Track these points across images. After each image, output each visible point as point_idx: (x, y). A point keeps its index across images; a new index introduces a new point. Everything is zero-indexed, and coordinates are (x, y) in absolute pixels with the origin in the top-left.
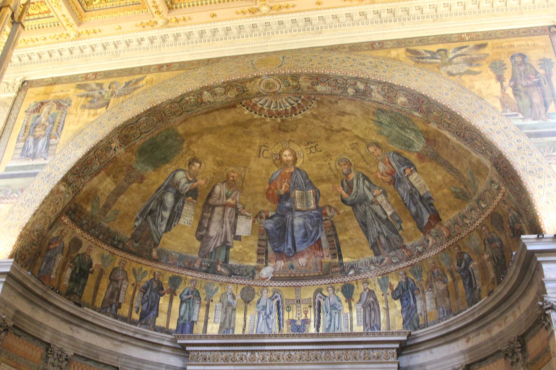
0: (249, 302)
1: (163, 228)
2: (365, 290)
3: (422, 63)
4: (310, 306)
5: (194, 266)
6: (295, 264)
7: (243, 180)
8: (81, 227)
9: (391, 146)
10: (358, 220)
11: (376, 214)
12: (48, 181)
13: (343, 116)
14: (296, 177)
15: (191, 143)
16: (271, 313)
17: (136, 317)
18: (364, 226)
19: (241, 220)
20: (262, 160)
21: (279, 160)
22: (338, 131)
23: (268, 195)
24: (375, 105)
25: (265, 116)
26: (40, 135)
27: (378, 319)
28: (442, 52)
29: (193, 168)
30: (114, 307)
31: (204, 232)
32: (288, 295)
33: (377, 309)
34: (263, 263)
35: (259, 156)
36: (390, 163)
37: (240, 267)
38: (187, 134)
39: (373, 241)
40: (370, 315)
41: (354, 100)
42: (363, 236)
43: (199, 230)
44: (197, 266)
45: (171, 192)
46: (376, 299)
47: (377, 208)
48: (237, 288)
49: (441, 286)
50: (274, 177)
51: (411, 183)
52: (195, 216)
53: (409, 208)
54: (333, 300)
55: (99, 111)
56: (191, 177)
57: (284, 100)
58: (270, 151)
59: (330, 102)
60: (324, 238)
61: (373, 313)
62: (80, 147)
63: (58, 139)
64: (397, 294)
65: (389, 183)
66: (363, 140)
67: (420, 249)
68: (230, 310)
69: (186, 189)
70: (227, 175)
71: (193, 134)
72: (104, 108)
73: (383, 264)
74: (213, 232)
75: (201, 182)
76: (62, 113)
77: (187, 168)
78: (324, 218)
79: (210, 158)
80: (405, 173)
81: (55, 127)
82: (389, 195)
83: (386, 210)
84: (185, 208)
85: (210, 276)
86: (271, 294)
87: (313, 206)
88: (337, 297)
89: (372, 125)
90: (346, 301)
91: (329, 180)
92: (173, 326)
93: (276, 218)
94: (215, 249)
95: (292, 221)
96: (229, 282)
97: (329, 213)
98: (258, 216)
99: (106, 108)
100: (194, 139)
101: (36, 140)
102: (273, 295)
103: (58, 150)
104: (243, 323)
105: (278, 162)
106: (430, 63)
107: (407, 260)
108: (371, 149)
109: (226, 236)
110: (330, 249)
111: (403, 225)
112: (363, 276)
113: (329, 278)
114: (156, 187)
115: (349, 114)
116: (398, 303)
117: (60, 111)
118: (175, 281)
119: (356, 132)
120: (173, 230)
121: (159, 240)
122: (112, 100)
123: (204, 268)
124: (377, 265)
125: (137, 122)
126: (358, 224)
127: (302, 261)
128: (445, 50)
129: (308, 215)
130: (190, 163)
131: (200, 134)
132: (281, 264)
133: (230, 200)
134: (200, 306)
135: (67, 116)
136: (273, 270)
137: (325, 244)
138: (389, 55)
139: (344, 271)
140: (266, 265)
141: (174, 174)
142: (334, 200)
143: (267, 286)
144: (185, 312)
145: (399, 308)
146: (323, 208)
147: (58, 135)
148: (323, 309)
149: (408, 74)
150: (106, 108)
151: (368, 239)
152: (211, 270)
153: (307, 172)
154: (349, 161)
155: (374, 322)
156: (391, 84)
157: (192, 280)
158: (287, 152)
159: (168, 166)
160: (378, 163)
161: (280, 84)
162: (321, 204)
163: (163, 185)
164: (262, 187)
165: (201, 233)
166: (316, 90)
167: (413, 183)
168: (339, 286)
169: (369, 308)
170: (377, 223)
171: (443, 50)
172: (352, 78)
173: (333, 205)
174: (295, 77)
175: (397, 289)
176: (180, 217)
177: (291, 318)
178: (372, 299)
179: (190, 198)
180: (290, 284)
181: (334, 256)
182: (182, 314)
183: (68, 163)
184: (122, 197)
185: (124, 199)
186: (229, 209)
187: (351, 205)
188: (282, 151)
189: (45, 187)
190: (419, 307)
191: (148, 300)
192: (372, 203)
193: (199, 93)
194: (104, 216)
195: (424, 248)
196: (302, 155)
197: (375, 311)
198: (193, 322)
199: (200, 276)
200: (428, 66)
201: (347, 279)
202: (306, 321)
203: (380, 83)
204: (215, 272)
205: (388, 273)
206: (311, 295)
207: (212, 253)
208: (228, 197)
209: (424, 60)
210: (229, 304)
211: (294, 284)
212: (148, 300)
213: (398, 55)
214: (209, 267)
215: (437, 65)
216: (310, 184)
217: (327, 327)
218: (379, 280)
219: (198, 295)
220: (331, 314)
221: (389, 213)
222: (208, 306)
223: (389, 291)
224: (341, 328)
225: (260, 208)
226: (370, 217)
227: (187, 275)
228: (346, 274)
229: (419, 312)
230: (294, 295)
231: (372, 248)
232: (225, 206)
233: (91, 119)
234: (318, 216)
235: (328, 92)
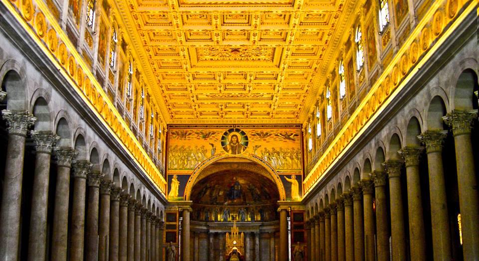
18: (252, 194)
21: (232, 179)
49: (270, 212)
74: (213, 195)
87: (239, 188)
92: (204, 219)
118: (204, 208)
120: (205, 196)
127: (235, 201)
132: (230, 201)
137: (242, 197)
139: (246, 205)
152: (212, 204)
201: (247, 206)
202: (236, 216)
219: (209, 210)
221: (259, 193)
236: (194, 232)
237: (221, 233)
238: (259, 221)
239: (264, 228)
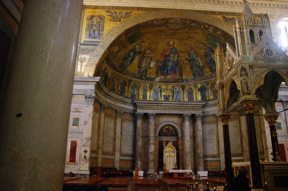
0: (151, 89)
1: (128, 64)
2: (189, 87)
3: (227, 22)
4: (170, 91)
5: (136, 77)
6: (167, 77)
7: (156, 49)
8: (107, 63)
9: (208, 45)
10: (190, 66)
11: (197, 65)
12: (103, 48)
13: (195, 33)
14: (173, 50)
15: (143, 36)
16: (158, 93)
17: (119, 93)
18: (192, 68)
19: (152, 62)
20: (163, 44)
21: (168, 44)
22: (192, 38)
23: (162, 55)
24: (208, 33)
25: (169, 30)
26: (95, 30)
27: (193, 97)
28: (233, 19)
29: (142, 44)
30: (114, 90)
31: (140, 65)
32: (164, 87)
33: (192, 94)
34: (156, 76)
35: (162, 42)
36: (206, 51)
37: (150, 77)
38: (143, 33)
39: (194, 73)
40: (190, 95)
41: (202, 30)
42: (191, 71)
43: (139, 65)
44: (137, 76)
45: (133, 52)
46: (192, 91)
47: (197, 63)
48: (148, 84)
50: (165, 49)
51: (211, 57)
52: (138, 60)
53: (209, 64)
54: (178, 90)
55: (117, 23)
56: (140, 47)
57: (178, 26)
58: (166, 41)
59: (193, 29)
60: (177, 70)
61: (191, 95)
62: (113, 36)
63: (103, 32)
64: (200, 90)
65: (204, 56)
66: (199, 42)
67: (209, 77)
68: (145, 91)
69: (138, 51)
70: (151, 47)
71: (145, 33)
72: (119, 22)
73: (196, 80)
74: (143, 66)
75: (143, 49)
76: (102, 21)
77: (140, 44)
78: (179, 64)
79: (147, 41)
80: (210, 54)
81: (101, 27)
82: (202, 59)
83: (200, 64)
84: (136, 57)
85: (140, 80)
86: (158, 87)
87: (176, 60)
88: (180, 89)
89: (204, 38)
90: (182, 90)
91: (183, 52)
92: (130, 96)
93: (163, 62)
94: (143, 71)
95: (168, 64)
96: (146, 82)
97: (181, 63)
98: (158, 61)
99: (120, 22)
100: (145, 35)
101: (94, 31)
102: (159, 87)
103: (104, 37)
104: (149, 95)
105: (168, 44)
106: (230, 22)
107: (204, 80)
108: (201, 45)
109: (147, 67)
110: (179, 74)
111: (205, 69)
112: (189, 83)
113: (177, 83)
114: (129, 50)
115: (198, 33)
116: (200, 92)
117: (101, 21)
118: (130, 81)
119: (198, 39)
120: (131, 64)
121: (127, 68)
122: (122, 19)
123: (139, 77)
124: (194, 80)
125: (131, 29)
126: (190, 67)
127: (169, 77)
128: (234, 18)
129: (174, 63)
130: (141, 43)
131: (147, 33)
132: (162, 77)
133: (150, 56)
134: (137, 90)
135: (105, 23)
136: (159, 79)
137: (177, 72)
138: (217, 17)
139: (183, 81)
140: (158, 77)
141: (135, 46)
142: (183, 59)
143: (157, 84)
144: (132, 91)
145: (200, 94)
146: (179, 61)
147: (103, 30)
148: (175, 92)
149: (223, 25)
150: (120, 22)
151: (192, 72)
152: (141, 78)
153: (177, 49)
154: (192, 47)
155: (191, 97)
156: (218, 28)
157: (135, 81)
158: (172, 42)
159: (134, 43)
160: (202, 49)
161: (180, 21)
162: (179, 59)
163: (131, 49)
164: (161, 52)
165: (139, 66)
166: (191, 25)
167: (213, 57)
168: (180, 86)
169: (190, 93)
170: (196, 67)
171: (233, 18)
172: (205, 23)
173: (183, 60)
174: (186, 20)
175: (199, 88)
176: (134, 60)
177: (164, 94)
178: (191, 90)
179: (138, 54)
180: (165, 84)
181: (180, 76)
182: (132, 92)
183: (109, 42)
184: (119, 53)
185: (119, 54)
186: (149, 58)
187: (188, 61)
188: (170, 41)
189: (102, 50)
190: (207, 94)
191: (122, 88)
192: (196, 61)
193: (153, 21)
194: (114, 59)
195: (211, 77)
196: (176, 43)
197: (192, 94)
198: (135, 95)
199: (137, 80)
200: (229, 23)
201: (183, 84)
203: (214, 26)
204: (142, 79)
205: (197, 83)
206: (171, 88)
207: (142, 72)
208: (149, 54)
209: (228, 21)
210: (145, 89)
211: (166, 84)
212: (122, 88)
213: (220, 18)
214: (140, 77)
215: (231, 23)
216: (177, 53)
217: (176, 98)
218: (194, 85)
219: (136, 85)
220: (177, 94)
221: (201, 65)
222: (139, 90)
223: (197, 88)
224: (181, 99)
225: (159, 59)
226: (194, 65)
227: (134, 79)
228: (183, 82)
229: (206, 96)
230: (166, 87)
231: (193, 75)
232: (148, 57)
233: (115, 26)
234: (177, 63)
235: (195, 26)
236: (116, 111)
237: (152, 114)
238: (200, 102)
239: (207, 109)
